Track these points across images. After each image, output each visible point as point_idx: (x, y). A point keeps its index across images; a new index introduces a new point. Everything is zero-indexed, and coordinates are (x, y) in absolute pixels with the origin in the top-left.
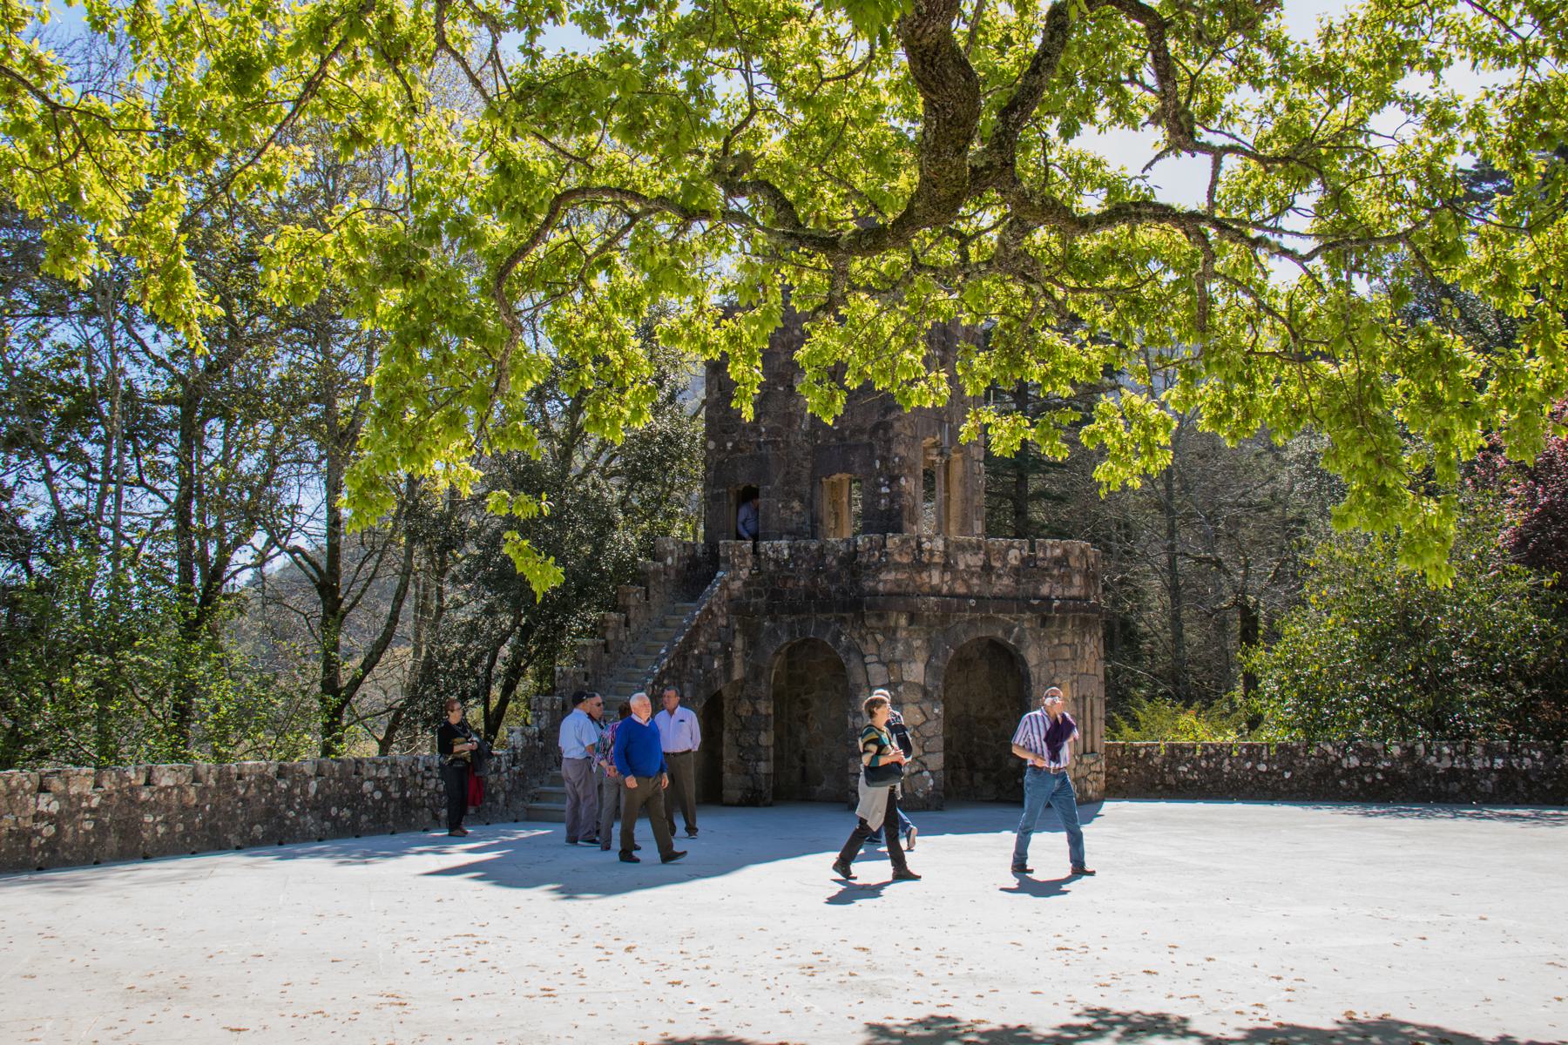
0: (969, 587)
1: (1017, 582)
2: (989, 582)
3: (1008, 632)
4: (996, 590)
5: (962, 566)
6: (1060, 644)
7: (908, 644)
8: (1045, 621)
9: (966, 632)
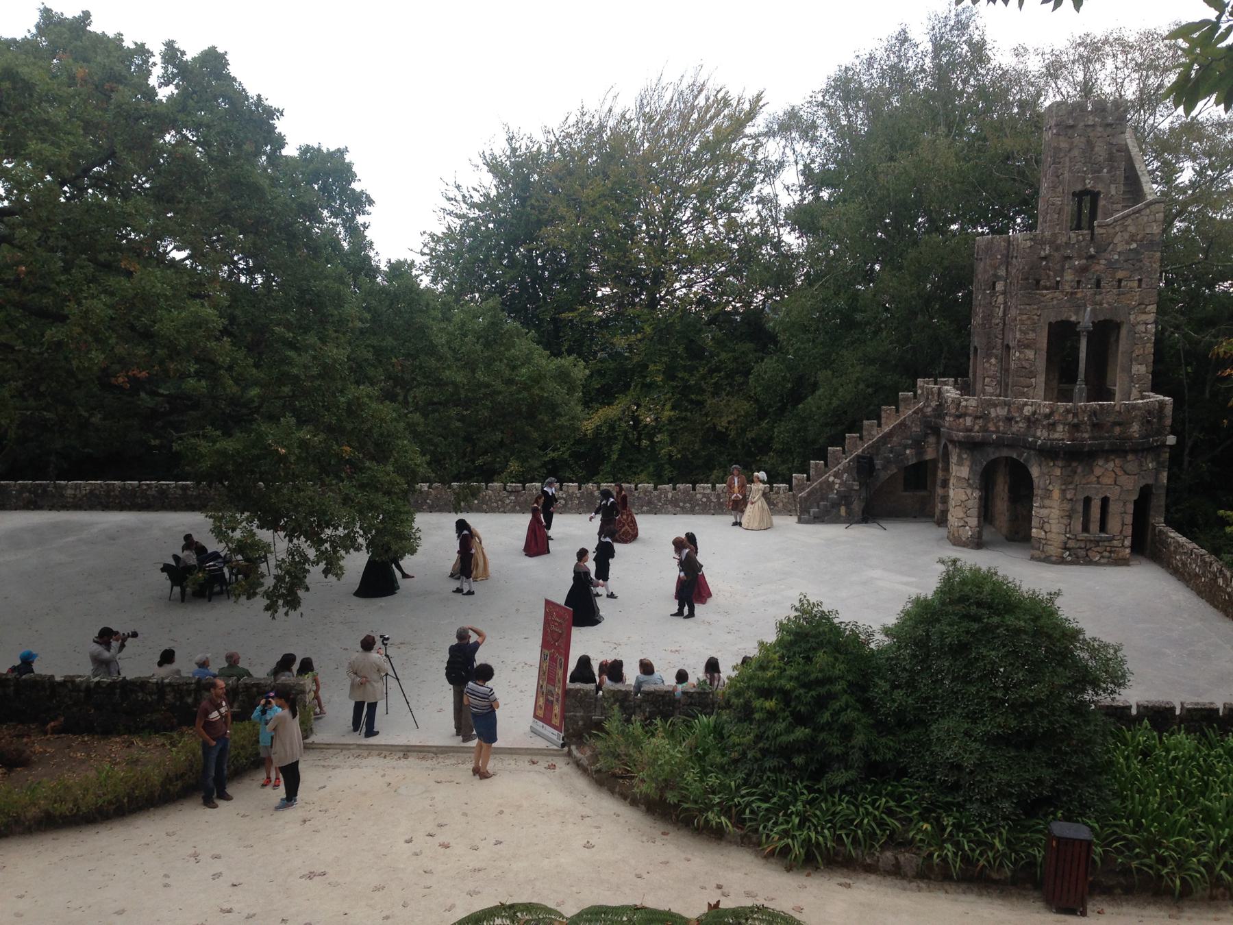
5: (993, 415)
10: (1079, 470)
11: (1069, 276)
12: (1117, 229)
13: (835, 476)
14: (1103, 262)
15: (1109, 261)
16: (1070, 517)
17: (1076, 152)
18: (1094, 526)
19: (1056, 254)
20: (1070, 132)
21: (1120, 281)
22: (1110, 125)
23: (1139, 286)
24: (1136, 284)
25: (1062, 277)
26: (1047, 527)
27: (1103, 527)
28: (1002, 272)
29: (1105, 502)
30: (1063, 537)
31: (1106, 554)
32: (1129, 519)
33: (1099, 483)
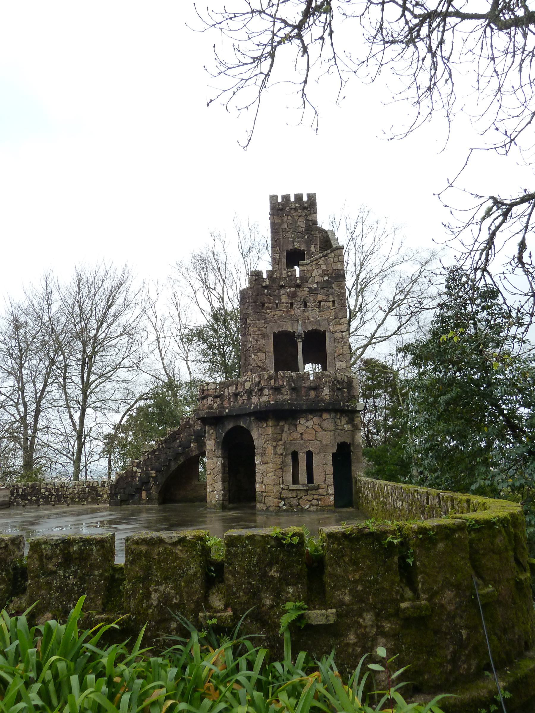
10: (286, 428)
11: (284, 299)
12: (314, 267)
13: (138, 467)
14: (307, 289)
15: (310, 288)
20: (280, 213)
21: (320, 302)
22: (305, 208)
23: (334, 306)
24: (331, 304)
25: (279, 300)
27: (310, 479)
29: (309, 455)
30: (277, 488)
31: (314, 502)
32: (330, 469)
33: (302, 439)
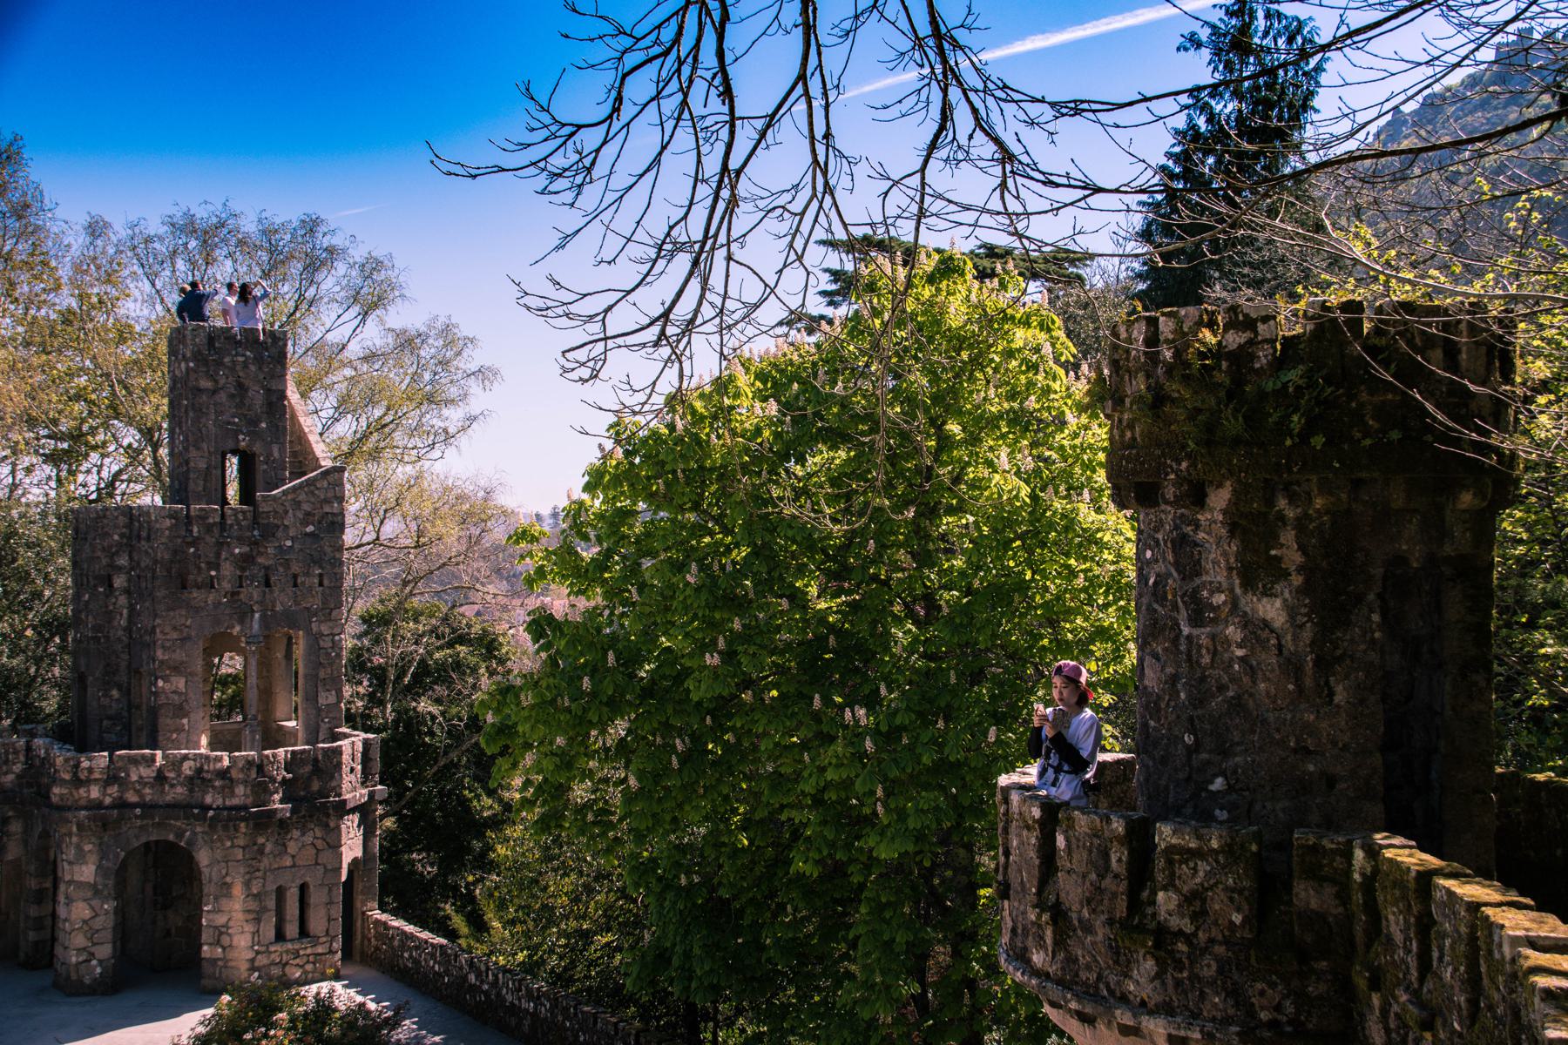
0: (142, 796)
1: (191, 791)
2: (163, 792)
3: (180, 835)
4: (168, 798)
5: (134, 778)
6: (233, 846)
7: (79, 847)
8: (212, 827)
9: (137, 837)
11: (228, 569)
16: (258, 920)
17: (222, 397)
18: (292, 929)
19: (208, 538)
21: (295, 577)
23: (321, 584)
26: (225, 940)
27: (304, 932)
28: (123, 561)
32: (337, 911)
